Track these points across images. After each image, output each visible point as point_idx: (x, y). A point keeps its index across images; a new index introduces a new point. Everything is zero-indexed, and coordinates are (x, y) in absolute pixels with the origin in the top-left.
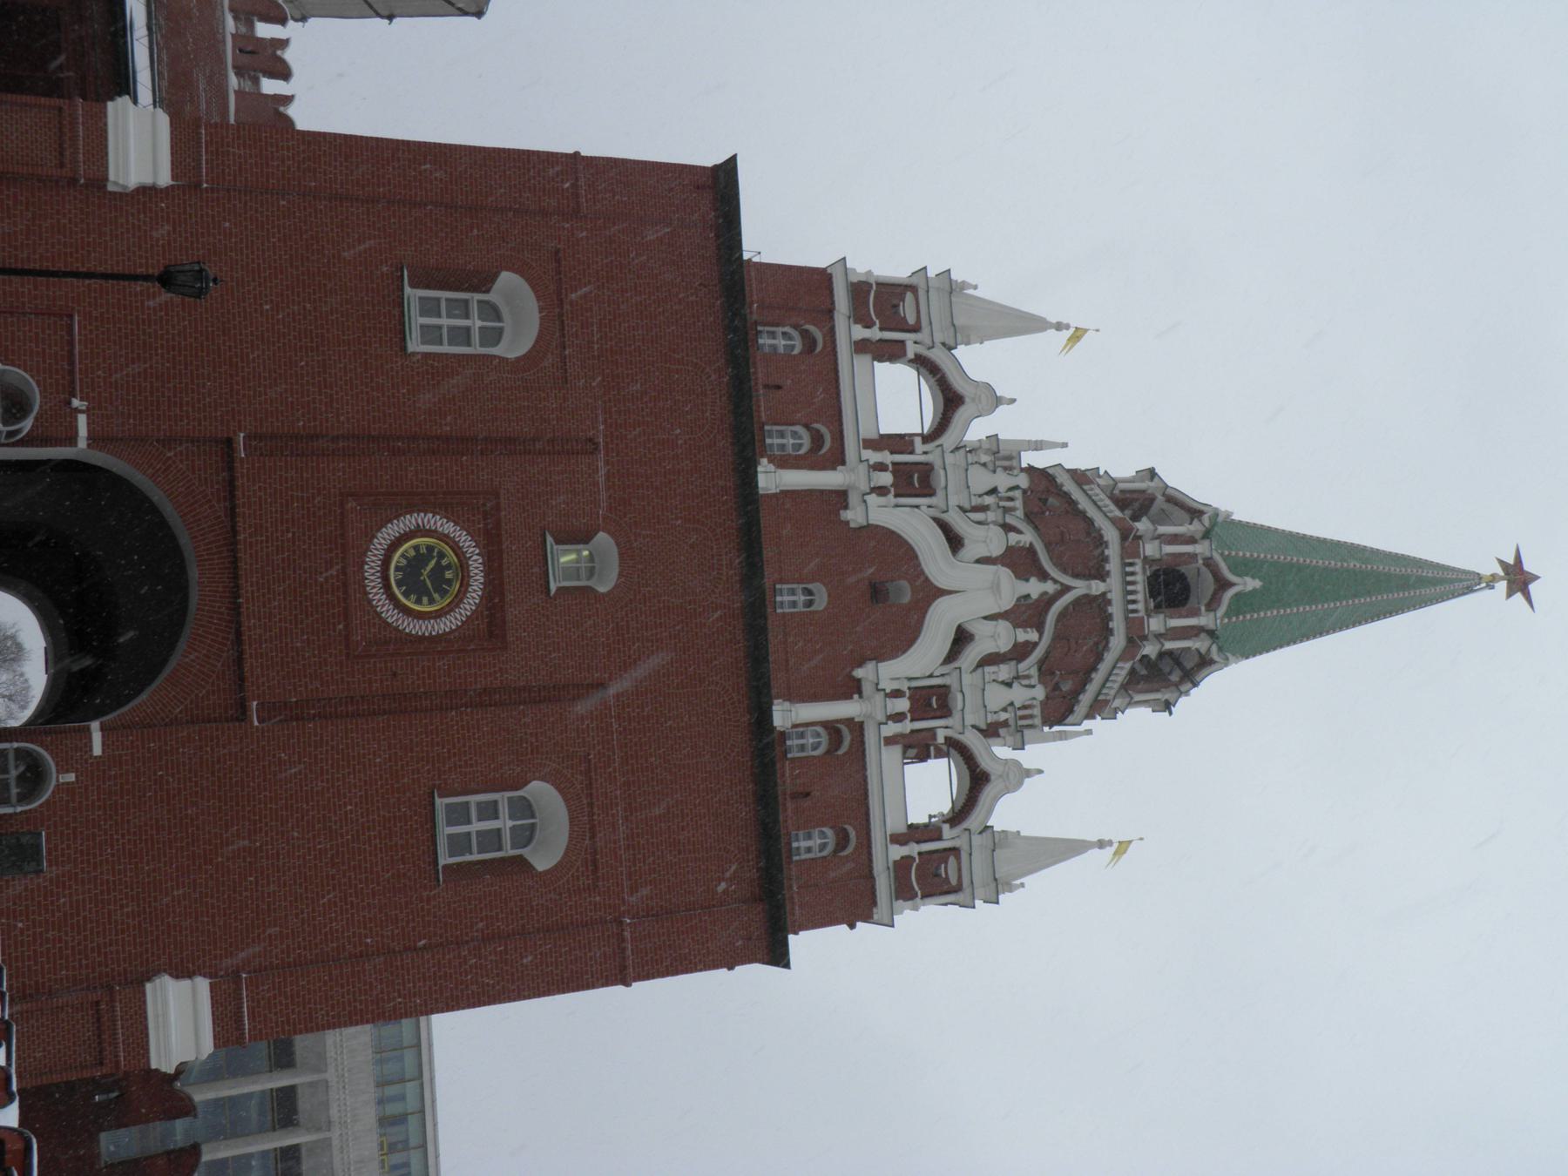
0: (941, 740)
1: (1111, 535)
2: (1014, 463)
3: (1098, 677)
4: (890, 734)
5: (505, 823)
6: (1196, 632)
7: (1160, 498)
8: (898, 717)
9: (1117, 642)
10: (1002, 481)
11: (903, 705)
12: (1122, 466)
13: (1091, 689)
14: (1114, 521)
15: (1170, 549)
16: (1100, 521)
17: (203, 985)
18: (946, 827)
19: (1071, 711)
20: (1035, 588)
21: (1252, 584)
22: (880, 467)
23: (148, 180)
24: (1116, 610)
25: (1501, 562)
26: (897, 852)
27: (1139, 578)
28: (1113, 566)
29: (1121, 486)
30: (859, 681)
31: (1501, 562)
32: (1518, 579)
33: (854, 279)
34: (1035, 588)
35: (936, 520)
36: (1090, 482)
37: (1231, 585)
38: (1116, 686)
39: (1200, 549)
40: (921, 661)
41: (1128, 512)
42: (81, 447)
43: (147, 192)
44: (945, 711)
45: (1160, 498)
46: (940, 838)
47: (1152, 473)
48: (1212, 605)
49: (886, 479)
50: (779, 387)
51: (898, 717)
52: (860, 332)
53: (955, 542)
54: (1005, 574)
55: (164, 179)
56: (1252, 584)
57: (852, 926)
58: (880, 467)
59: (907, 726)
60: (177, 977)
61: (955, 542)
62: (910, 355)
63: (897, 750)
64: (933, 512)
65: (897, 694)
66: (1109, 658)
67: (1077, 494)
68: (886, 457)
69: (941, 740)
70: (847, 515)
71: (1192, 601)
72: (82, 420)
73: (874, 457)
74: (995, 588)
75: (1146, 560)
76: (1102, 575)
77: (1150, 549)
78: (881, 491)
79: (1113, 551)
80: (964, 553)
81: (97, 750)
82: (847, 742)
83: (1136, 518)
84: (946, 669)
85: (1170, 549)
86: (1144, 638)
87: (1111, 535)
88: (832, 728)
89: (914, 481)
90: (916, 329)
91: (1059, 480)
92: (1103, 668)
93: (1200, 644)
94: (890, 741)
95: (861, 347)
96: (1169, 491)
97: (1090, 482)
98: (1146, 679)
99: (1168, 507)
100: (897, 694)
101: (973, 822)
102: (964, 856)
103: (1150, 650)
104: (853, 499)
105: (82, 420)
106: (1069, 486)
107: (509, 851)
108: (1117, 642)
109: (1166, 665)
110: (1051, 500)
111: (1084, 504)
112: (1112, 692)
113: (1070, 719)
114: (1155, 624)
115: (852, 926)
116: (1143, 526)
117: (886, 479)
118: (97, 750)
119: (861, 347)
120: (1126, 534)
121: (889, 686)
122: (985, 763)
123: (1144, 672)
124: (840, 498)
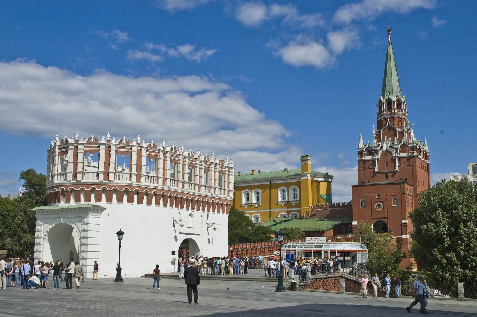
1: (383, 117)
7: (380, 105)
12: (377, 109)
15: (385, 109)
33: (358, 159)
34: (385, 138)
40: (392, 151)
44: (397, 148)
47: (377, 105)
52: (363, 157)
53: (382, 147)
54: (384, 142)
55: (356, 222)
59: (398, 153)
68: (374, 155)
73: (374, 157)
74: (385, 143)
76: (388, 118)
78: (377, 156)
80: (382, 146)
82: (400, 159)
86: (395, 111)
87: (383, 117)
88: (399, 160)
89: (376, 151)
94: (400, 155)
95: (364, 158)
106: (379, 119)
117: (376, 155)
119: (364, 158)
122: (402, 143)
124: (378, 160)
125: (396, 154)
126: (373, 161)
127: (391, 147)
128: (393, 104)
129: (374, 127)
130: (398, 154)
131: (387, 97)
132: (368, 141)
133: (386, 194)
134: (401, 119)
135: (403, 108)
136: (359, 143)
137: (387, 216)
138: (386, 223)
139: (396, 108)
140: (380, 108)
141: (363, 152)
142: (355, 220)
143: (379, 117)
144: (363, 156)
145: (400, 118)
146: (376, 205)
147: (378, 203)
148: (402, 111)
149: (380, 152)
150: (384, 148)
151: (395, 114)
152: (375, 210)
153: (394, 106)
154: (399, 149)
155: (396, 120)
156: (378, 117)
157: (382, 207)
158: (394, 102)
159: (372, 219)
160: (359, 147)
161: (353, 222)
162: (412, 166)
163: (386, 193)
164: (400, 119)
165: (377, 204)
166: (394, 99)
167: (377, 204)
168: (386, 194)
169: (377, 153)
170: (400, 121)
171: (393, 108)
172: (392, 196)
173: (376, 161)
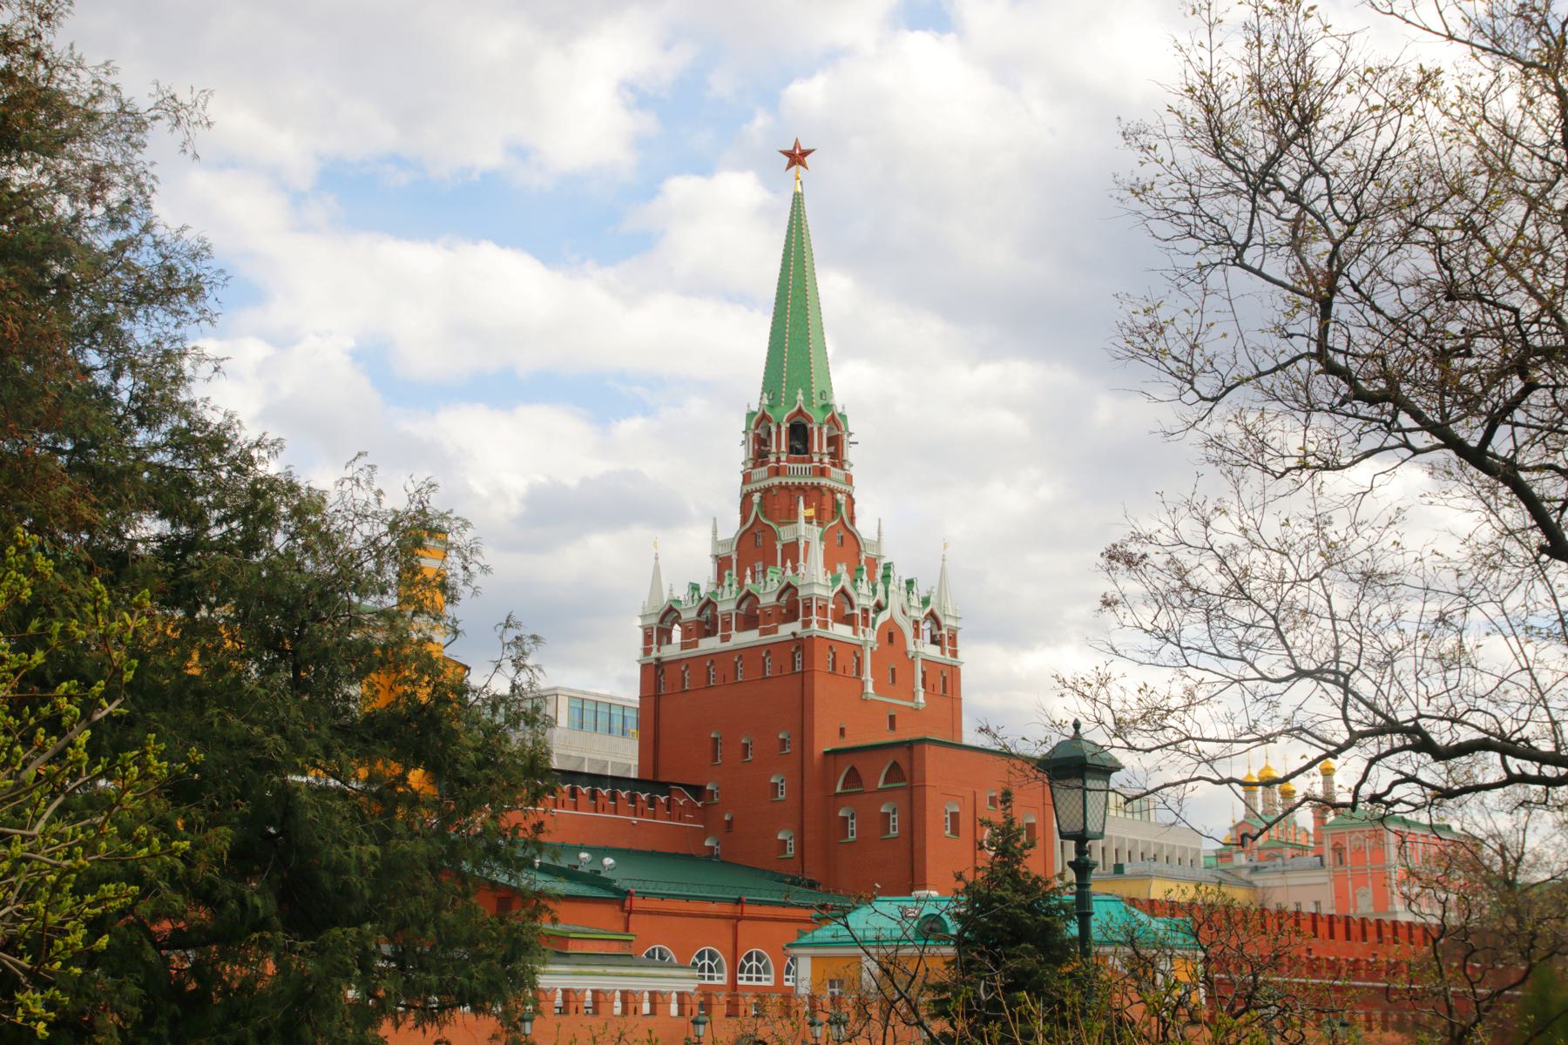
1: (776, 481)
6: (820, 429)
9: (823, 481)
14: (770, 476)
21: (800, 397)
25: (790, 166)
28: (790, 482)
31: (790, 166)
32: (797, 157)
37: (800, 411)
39: (783, 429)
48: (810, 420)
56: (800, 397)
75: (788, 461)
77: (783, 458)
79: (784, 480)
85: (783, 448)
86: (821, 461)
87: (776, 481)
93: (825, 430)
108: (823, 481)
114: (816, 459)
116: (772, 458)
139: (825, 450)
143: (754, 478)
148: (842, 468)
156: (747, 478)
166: (817, 417)
171: (816, 449)
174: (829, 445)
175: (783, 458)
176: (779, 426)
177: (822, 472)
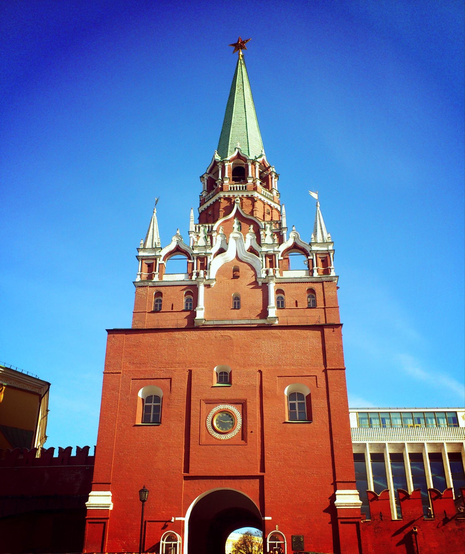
0: (282, 258)
1: (222, 194)
2: (197, 226)
3: (266, 200)
4: (279, 275)
5: (296, 402)
7: (211, 175)
8: (275, 271)
10: (202, 235)
11: (271, 270)
12: (200, 187)
13: (270, 202)
15: (227, 176)
16: (216, 197)
17: (338, 492)
18: (309, 258)
19: (277, 209)
20: (236, 226)
22: (198, 274)
23: (110, 498)
24: (245, 195)
26: (316, 274)
27: (235, 186)
28: (231, 195)
29: (206, 189)
30: (262, 283)
35: (214, 257)
36: (204, 199)
38: (269, 194)
39: (226, 164)
41: (214, 186)
42: (186, 519)
43: (112, 501)
45: (211, 175)
46: (312, 260)
47: (202, 177)
48: (245, 160)
49: (202, 272)
50: (172, 305)
51: (275, 271)
52: (156, 279)
53: (222, 251)
54: (232, 235)
55: (109, 493)
57: (338, 288)
58: (198, 274)
59: (277, 268)
60: (335, 499)
61: (222, 251)
62: (163, 262)
63: (284, 272)
64: (212, 256)
65: (267, 272)
66: (260, 197)
67: (208, 204)
69: (282, 258)
70: (213, 284)
71: (244, 166)
72: (177, 519)
73: (194, 277)
74: (236, 238)
78: (205, 273)
81: (270, 518)
83: (216, 185)
84: (260, 255)
86: (254, 184)
90: (156, 260)
91: (203, 210)
92: (263, 198)
95: (160, 277)
96: (207, 172)
97: (204, 199)
98: (268, 183)
99: (214, 171)
100: (267, 272)
101: (308, 249)
102: (318, 252)
103: (258, 182)
104: (207, 283)
105: (177, 519)
106: (205, 206)
107: (305, 401)
108: (256, 194)
109: (264, 176)
110: (210, 213)
111: (211, 202)
112: (271, 195)
113: (279, 209)
114: (250, 181)
115: (338, 288)
117: (202, 272)
118: (270, 518)
119: (160, 277)
120: (222, 190)
121: (264, 275)
123: (265, 184)
125: (271, 270)
126: (192, 292)
127: (252, 250)
128: (250, 167)
129: (192, 214)
130: (277, 272)
131: (231, 155)
132: (178, 232)
133: (260, 371)
134: (269, 208)
135: (274, 187)
136: (147, 237)
137: (263, 469)
138: (257, 504)
139: (257, 176)
140: (212, 184)
141: (158, 262)
142: (103, 486)
144: (157, 272)
145: (270, 206)
146: (210, 418)
147: (222, 407)
149: (216, 264)
150: (230, 255)
151: (255, 189)
152: (203, 440)
153: (253, 172)
154: (279, 257)
155: (258, 205)
156: (202, 203)
157: (239, 426)
158: (253, 162)
159: (186, 478)
160: (145, 244)
161: (92, 493)
162: (324, 308)
163: (257, 365)
164: (267, 207)
165: (215, 410)
167: (215, 410)
168: (260, 371)
169: (205, 267)
170: (269, 213)
171: (250, 175)
172: (286, 377)
173: (202, 289)
174: (261, 178)
175: (226, 182)
176: (223, 163)
177: (255, 189)
